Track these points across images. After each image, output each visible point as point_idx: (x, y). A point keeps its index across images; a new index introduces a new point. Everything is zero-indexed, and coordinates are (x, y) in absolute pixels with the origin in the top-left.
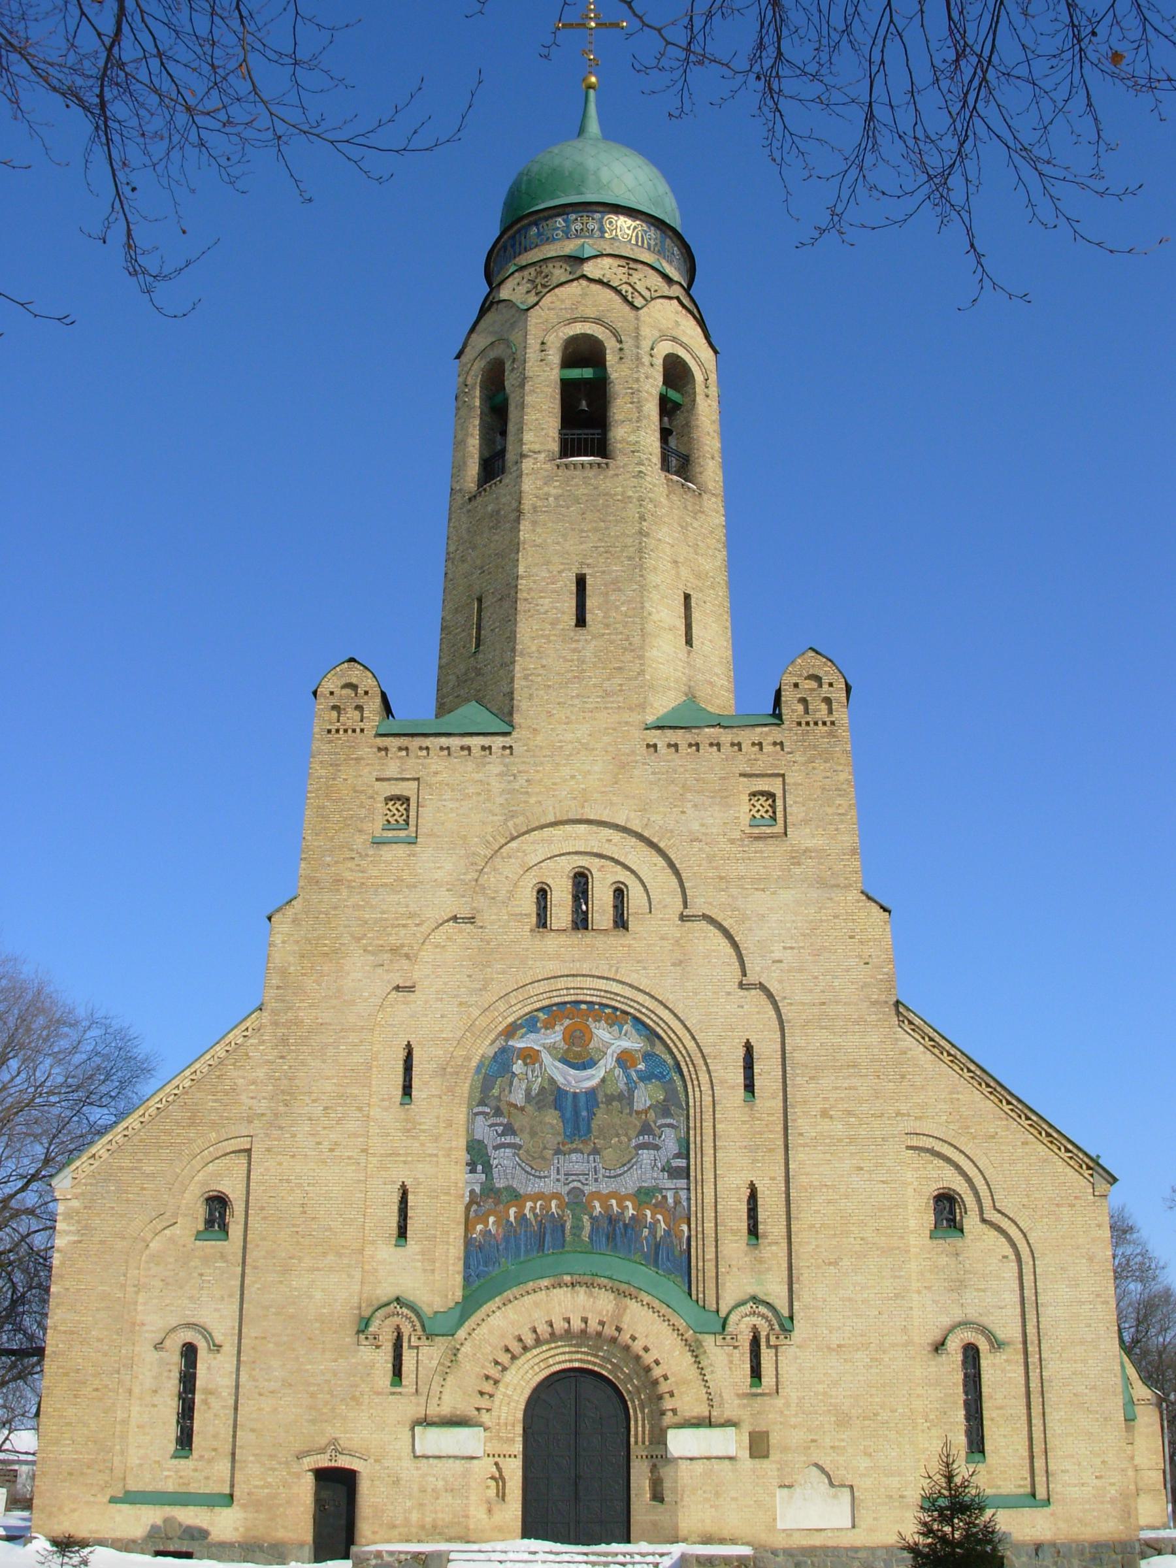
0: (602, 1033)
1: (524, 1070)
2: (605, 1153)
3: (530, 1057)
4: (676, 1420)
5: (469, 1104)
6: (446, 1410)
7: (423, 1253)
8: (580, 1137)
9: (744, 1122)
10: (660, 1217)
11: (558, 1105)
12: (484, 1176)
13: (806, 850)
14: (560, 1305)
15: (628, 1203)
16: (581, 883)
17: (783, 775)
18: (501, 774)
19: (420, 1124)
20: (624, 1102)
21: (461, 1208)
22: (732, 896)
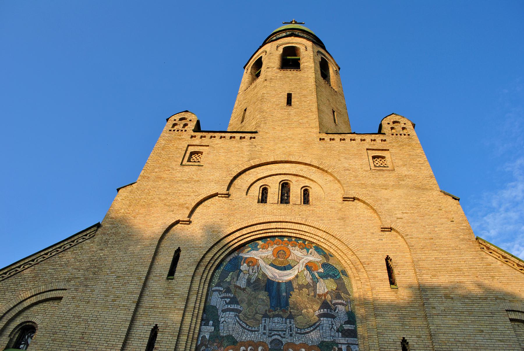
0: (296, 252)
8: (281, 308)
12: (213, 328)
13: (405, 176)
16: (285, 187)
18: (250, 145)
20: (310, 289)
22: (370, 191)
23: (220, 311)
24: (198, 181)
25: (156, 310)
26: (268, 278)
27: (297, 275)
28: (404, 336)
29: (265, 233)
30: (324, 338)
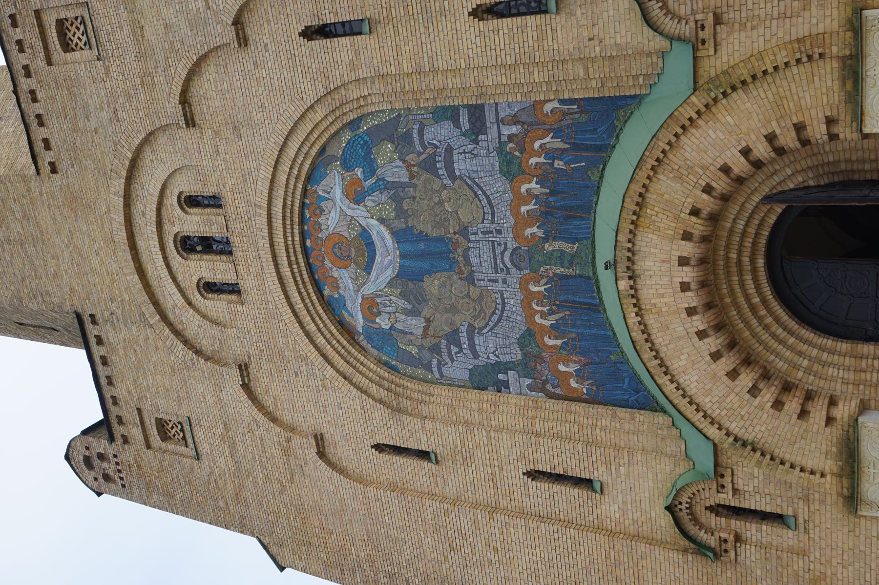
1: (386, 316)
2: (464, 220)
3: (371, 307)
4: (845, 118)
5: (432, 382)
6: (830, 465)
7: (608, 464)
8: (450, 252)
9: (397, 33)
10: (537, 145)
11: (418, 277)
14: (662, 296)
15: (524, 188)
16: (188, 245)
17: (37, 12)
19: (456, 447)
21: (551, 404)
22: (156, 67)
23: (477, 361)
24: (225, 424)
25: (498, 476)
26: (397, 276)
27: (378, 220)
28: (466, 13)
29: (305, 287)
30: (493, 169)
